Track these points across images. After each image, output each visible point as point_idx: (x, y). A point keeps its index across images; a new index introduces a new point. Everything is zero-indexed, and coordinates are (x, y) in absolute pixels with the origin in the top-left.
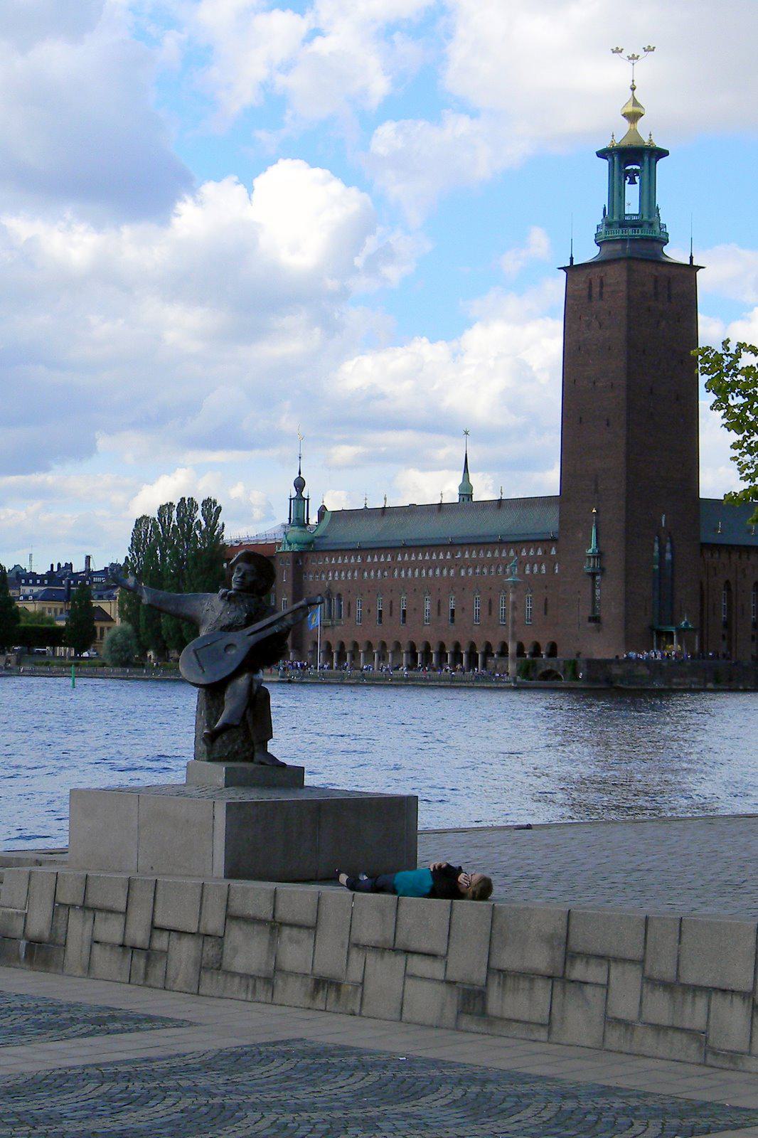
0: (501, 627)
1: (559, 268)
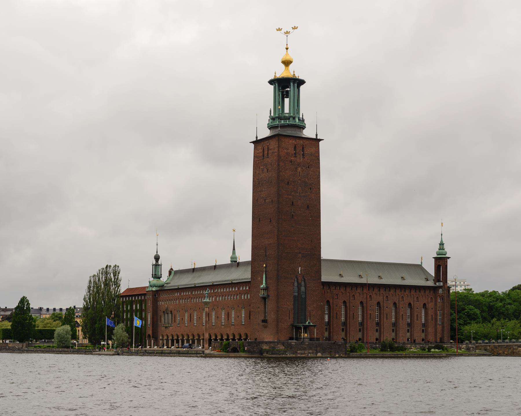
0: (232, 326)
1: (251, 142)
